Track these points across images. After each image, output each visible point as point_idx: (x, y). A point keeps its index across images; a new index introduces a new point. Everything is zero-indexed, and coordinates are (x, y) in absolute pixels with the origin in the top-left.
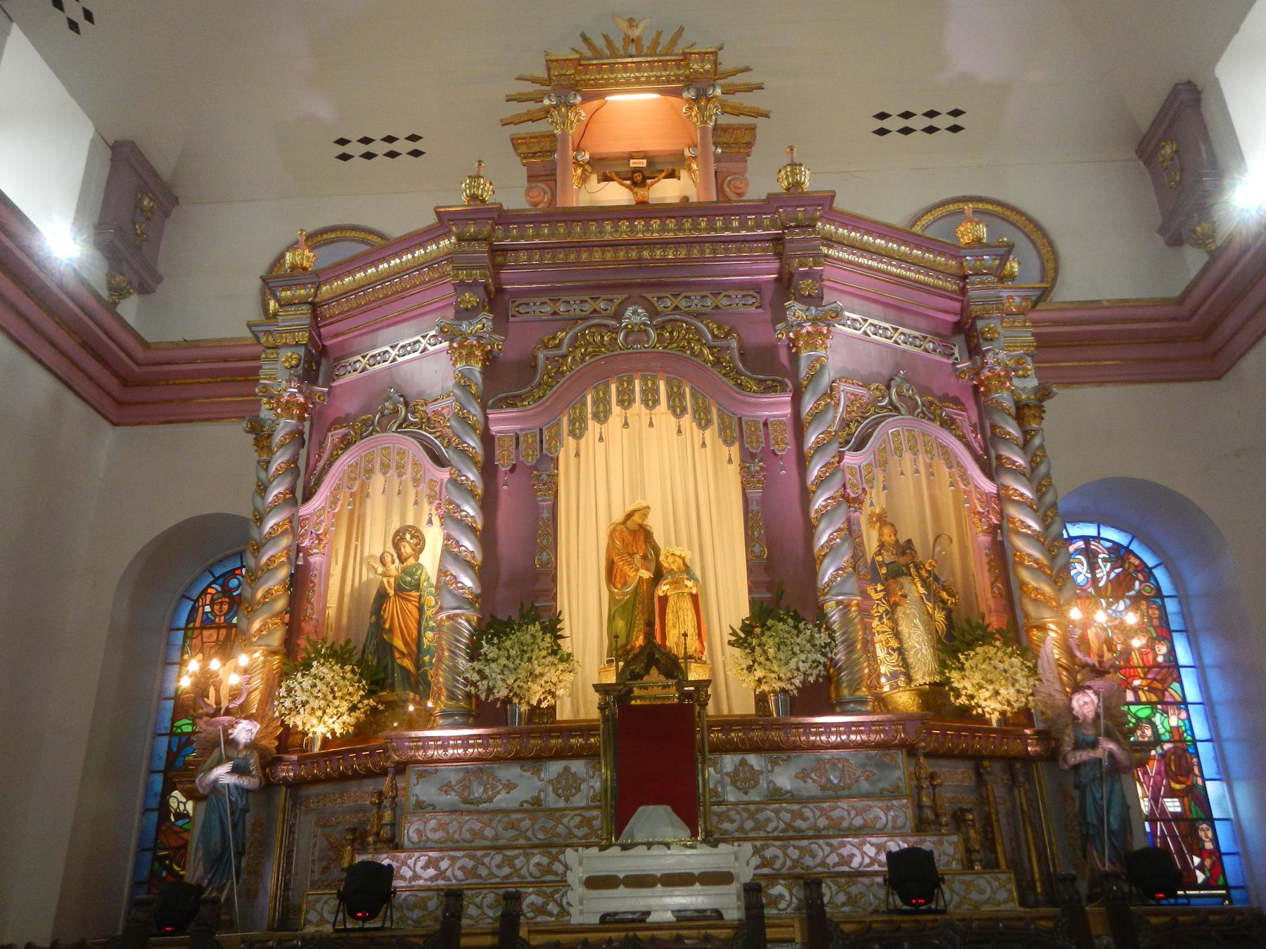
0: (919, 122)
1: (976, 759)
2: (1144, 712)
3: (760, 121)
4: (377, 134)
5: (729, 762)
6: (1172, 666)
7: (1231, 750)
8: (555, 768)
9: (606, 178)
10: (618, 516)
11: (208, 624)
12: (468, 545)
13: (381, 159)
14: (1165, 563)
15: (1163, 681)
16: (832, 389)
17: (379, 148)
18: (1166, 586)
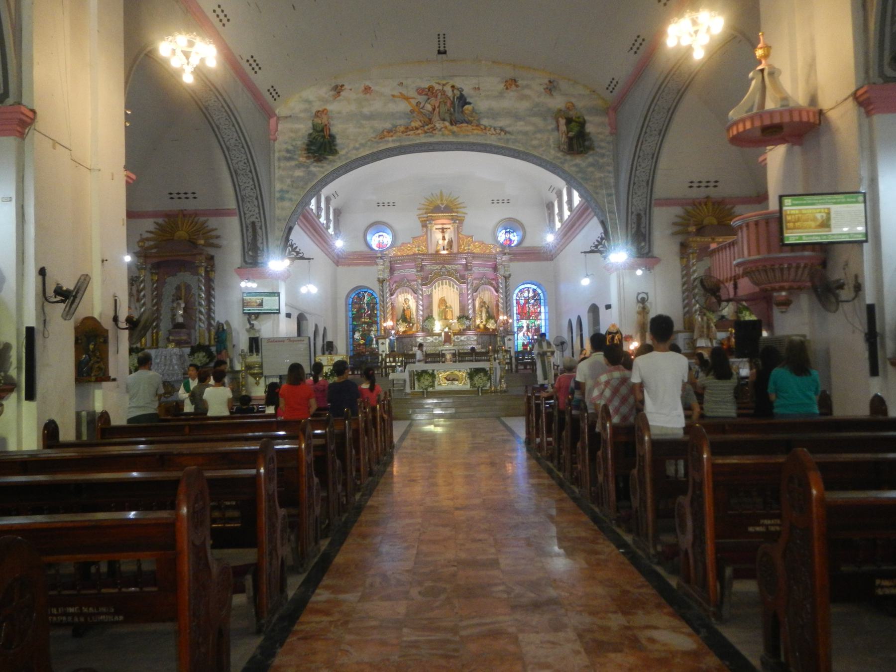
0: (501, 201)
1: (490, 335)
2: (533, 321)
3: (465, 215)
4: (386, 202)
5: (456, 336)
6: (540, 313)
7: (547, 327)
8: (434, 337)
9: (436, 229)
10: (440, 298)
11: (356, 303)
12: (421, 308)
13: (386, 206)
14: (543, 292)
15: (538, 315)
16: (473, 283)
17: (386, 204)
18: (542, 298)
